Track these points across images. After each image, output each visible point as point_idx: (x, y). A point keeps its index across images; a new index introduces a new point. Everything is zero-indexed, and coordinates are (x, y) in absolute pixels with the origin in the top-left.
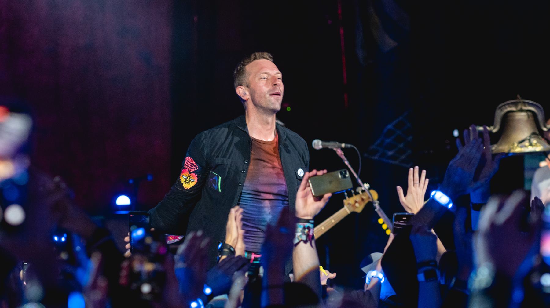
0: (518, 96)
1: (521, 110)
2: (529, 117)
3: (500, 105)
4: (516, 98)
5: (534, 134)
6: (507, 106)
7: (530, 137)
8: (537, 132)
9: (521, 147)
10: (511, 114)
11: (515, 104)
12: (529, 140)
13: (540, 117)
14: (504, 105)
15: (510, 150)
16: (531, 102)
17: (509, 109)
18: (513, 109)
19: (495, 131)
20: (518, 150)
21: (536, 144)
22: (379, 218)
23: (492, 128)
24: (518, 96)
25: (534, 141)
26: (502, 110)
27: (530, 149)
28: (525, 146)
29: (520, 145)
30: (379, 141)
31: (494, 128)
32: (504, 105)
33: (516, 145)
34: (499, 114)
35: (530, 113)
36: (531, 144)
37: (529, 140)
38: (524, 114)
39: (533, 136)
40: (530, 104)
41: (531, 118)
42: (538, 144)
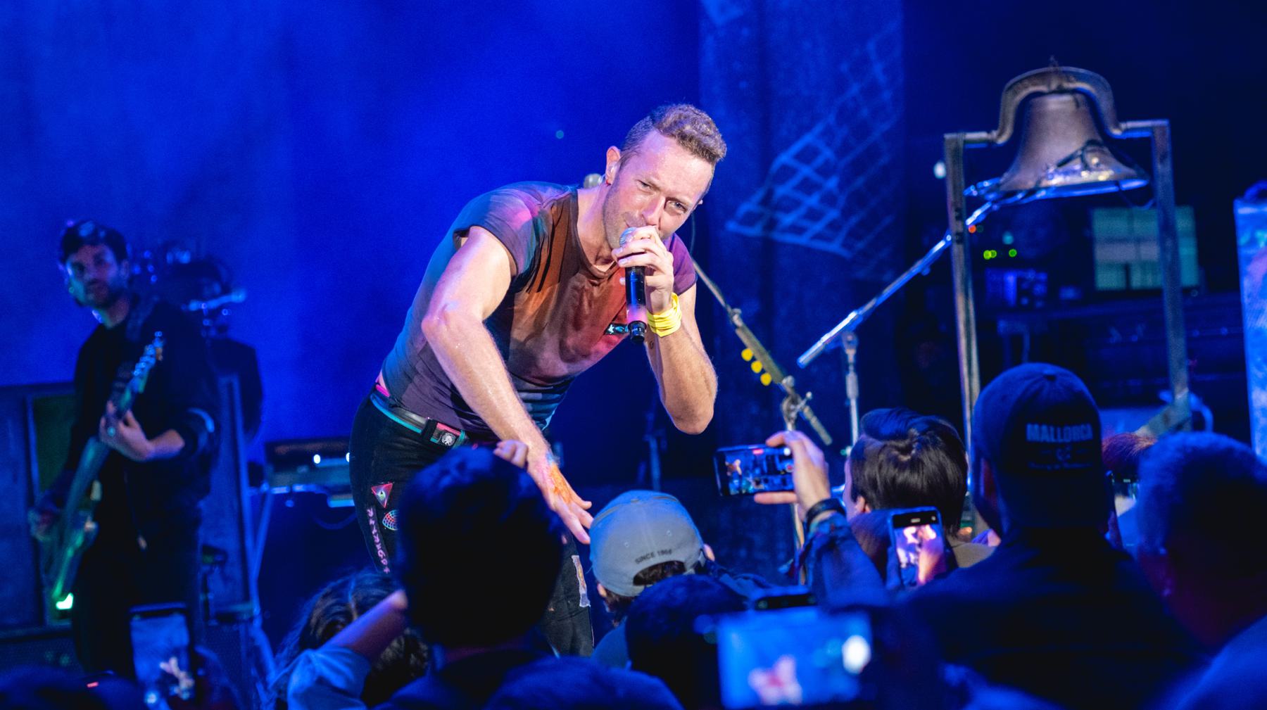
0: (1052, 59)
1: (1061, 91)
2: (1078, 105)
3: (1012, 81)
5: (1091, 142)
6: (1026, 82)
7: (1083, 149)
8: (1099, 139)
9: (1066, 173)
10: (1037, 100)
11: (1043, 77)
12: (1082, 157)
13: (1106, 104)
14: (1021, 81)
15: (1039, 182)
16: (1082, 71)
17: (1032, 89)
18: (1043, 88)
19: (1002, 140)
20: (1057, 181)
21: (1098, 165)
22: (743, 347)
23: (995, 133)
24: (1052, 59)
25: (1095, 160)
26: (1016, 93)
27: (1086, 176)
28: (1074, 172)
29: (1061, 170)
31: (1000, 135)
32: (1021, 81)
33: (1051, 170)
34: (1011, 102)
35: (1079, 96)
36: (1086, 167)
37: (1082, 157)
39: (1089, 148)
40: (1080, 78)
41: (1083, 108)
42: (1102, 166)
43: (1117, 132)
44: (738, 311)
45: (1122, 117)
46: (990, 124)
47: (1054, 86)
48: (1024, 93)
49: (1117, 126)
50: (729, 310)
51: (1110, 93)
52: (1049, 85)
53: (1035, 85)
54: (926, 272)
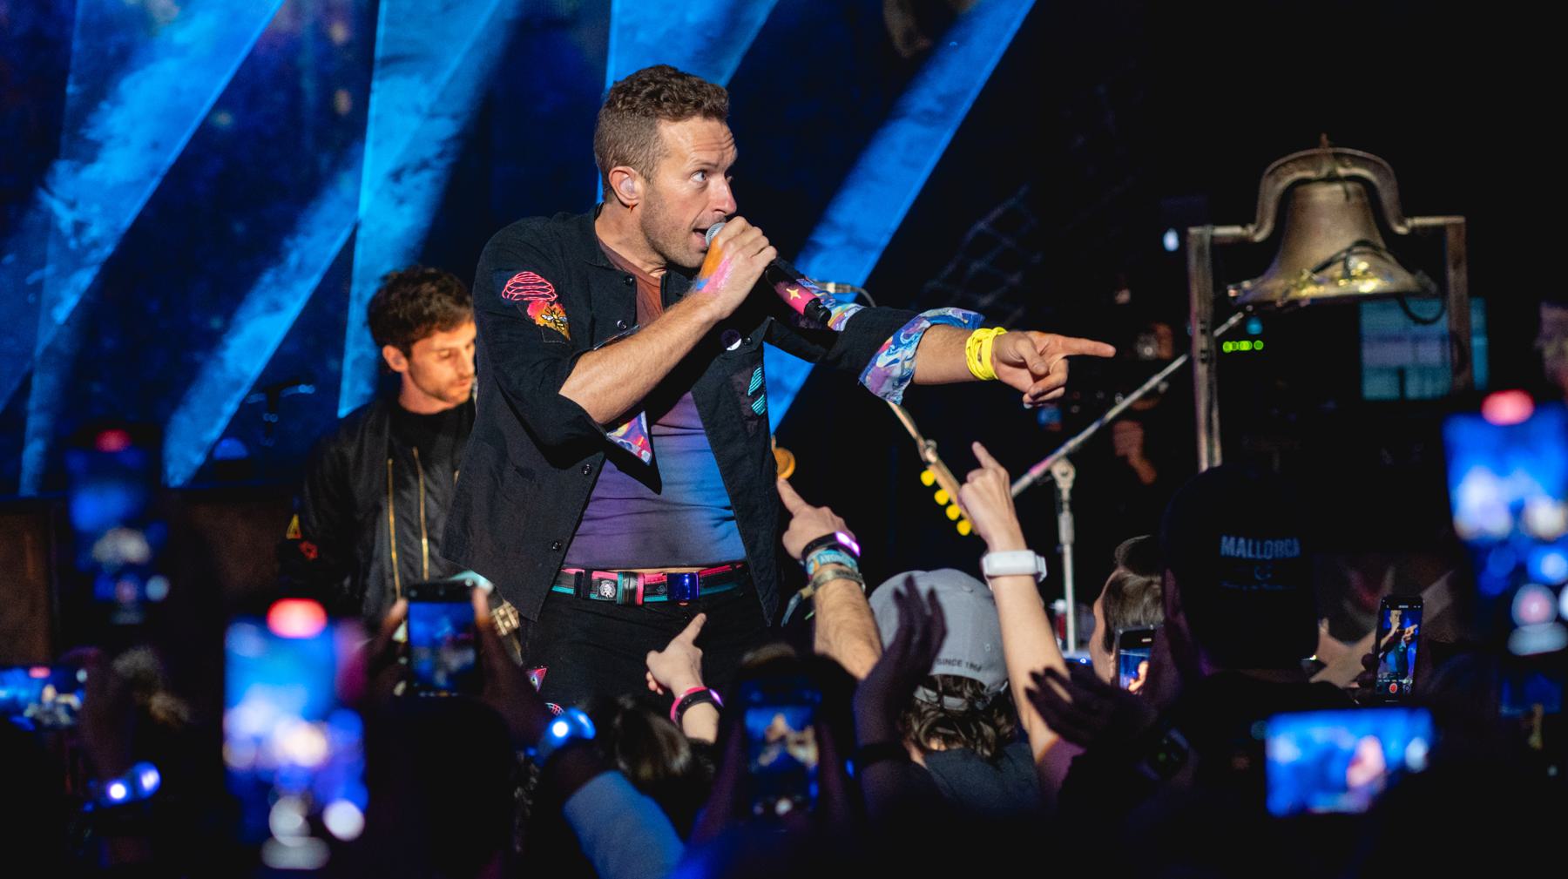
0: (1324, 137)
1: (1332, 179)
4: (1317, 145)
6: (1291, 166)
10: (1300, 189)
13: (1388, 196)
14: (1284, 165)
16: (1360, 153)
17: (1298, 175)
18: (1310, 174)
19: (1259, 237)
23: (1251, 229)
24: (1324, 137)
26: (1278, 180)
30: (951, 268)
31: (1257, 231)
32: (1284, 165)
34: (1272, 190)
38: (1338, 187)
40: (1357, 161)
43: (1401, 230)
44: (932, 443)
45: (1407, 212)
46: (1246, 216)
47: (1324, 172)
48: (1288, 180)
49: (1401, 223)
50: (921, 442)
51: (1393, 182)
52: (1319, 169)
53: (1301, 170)
54: (1163, 387)
